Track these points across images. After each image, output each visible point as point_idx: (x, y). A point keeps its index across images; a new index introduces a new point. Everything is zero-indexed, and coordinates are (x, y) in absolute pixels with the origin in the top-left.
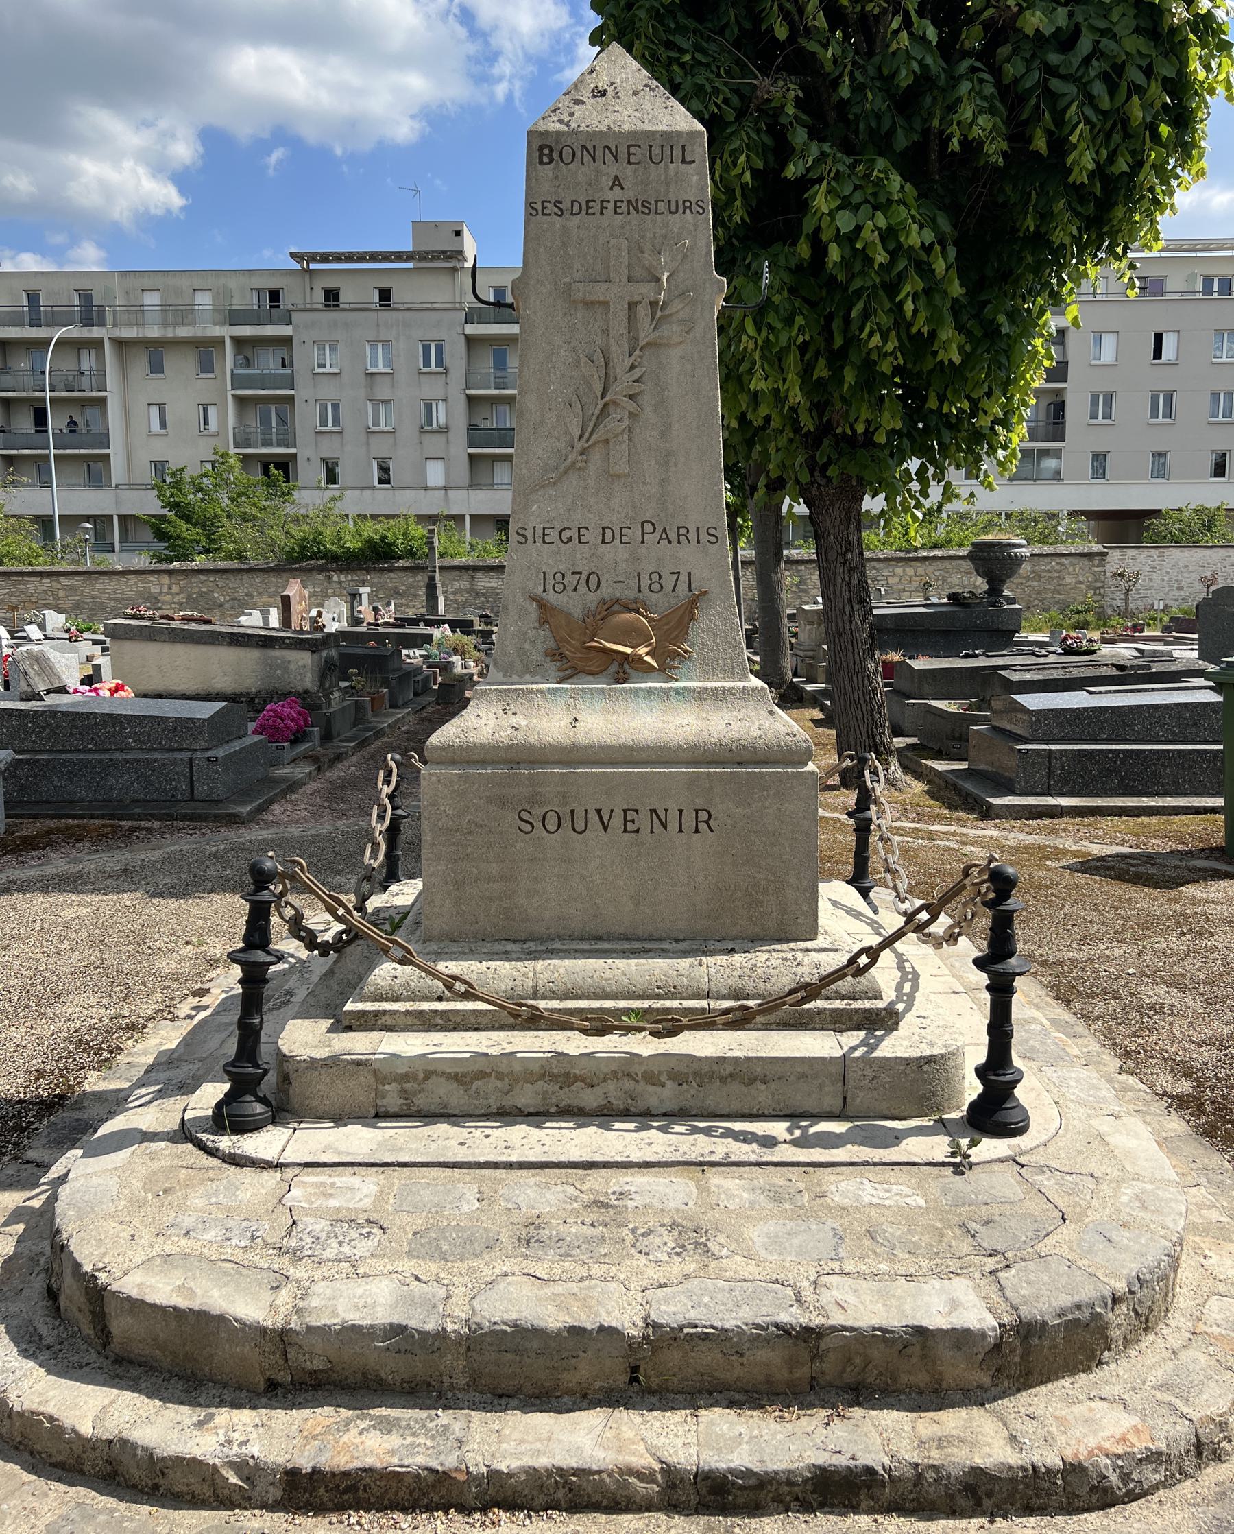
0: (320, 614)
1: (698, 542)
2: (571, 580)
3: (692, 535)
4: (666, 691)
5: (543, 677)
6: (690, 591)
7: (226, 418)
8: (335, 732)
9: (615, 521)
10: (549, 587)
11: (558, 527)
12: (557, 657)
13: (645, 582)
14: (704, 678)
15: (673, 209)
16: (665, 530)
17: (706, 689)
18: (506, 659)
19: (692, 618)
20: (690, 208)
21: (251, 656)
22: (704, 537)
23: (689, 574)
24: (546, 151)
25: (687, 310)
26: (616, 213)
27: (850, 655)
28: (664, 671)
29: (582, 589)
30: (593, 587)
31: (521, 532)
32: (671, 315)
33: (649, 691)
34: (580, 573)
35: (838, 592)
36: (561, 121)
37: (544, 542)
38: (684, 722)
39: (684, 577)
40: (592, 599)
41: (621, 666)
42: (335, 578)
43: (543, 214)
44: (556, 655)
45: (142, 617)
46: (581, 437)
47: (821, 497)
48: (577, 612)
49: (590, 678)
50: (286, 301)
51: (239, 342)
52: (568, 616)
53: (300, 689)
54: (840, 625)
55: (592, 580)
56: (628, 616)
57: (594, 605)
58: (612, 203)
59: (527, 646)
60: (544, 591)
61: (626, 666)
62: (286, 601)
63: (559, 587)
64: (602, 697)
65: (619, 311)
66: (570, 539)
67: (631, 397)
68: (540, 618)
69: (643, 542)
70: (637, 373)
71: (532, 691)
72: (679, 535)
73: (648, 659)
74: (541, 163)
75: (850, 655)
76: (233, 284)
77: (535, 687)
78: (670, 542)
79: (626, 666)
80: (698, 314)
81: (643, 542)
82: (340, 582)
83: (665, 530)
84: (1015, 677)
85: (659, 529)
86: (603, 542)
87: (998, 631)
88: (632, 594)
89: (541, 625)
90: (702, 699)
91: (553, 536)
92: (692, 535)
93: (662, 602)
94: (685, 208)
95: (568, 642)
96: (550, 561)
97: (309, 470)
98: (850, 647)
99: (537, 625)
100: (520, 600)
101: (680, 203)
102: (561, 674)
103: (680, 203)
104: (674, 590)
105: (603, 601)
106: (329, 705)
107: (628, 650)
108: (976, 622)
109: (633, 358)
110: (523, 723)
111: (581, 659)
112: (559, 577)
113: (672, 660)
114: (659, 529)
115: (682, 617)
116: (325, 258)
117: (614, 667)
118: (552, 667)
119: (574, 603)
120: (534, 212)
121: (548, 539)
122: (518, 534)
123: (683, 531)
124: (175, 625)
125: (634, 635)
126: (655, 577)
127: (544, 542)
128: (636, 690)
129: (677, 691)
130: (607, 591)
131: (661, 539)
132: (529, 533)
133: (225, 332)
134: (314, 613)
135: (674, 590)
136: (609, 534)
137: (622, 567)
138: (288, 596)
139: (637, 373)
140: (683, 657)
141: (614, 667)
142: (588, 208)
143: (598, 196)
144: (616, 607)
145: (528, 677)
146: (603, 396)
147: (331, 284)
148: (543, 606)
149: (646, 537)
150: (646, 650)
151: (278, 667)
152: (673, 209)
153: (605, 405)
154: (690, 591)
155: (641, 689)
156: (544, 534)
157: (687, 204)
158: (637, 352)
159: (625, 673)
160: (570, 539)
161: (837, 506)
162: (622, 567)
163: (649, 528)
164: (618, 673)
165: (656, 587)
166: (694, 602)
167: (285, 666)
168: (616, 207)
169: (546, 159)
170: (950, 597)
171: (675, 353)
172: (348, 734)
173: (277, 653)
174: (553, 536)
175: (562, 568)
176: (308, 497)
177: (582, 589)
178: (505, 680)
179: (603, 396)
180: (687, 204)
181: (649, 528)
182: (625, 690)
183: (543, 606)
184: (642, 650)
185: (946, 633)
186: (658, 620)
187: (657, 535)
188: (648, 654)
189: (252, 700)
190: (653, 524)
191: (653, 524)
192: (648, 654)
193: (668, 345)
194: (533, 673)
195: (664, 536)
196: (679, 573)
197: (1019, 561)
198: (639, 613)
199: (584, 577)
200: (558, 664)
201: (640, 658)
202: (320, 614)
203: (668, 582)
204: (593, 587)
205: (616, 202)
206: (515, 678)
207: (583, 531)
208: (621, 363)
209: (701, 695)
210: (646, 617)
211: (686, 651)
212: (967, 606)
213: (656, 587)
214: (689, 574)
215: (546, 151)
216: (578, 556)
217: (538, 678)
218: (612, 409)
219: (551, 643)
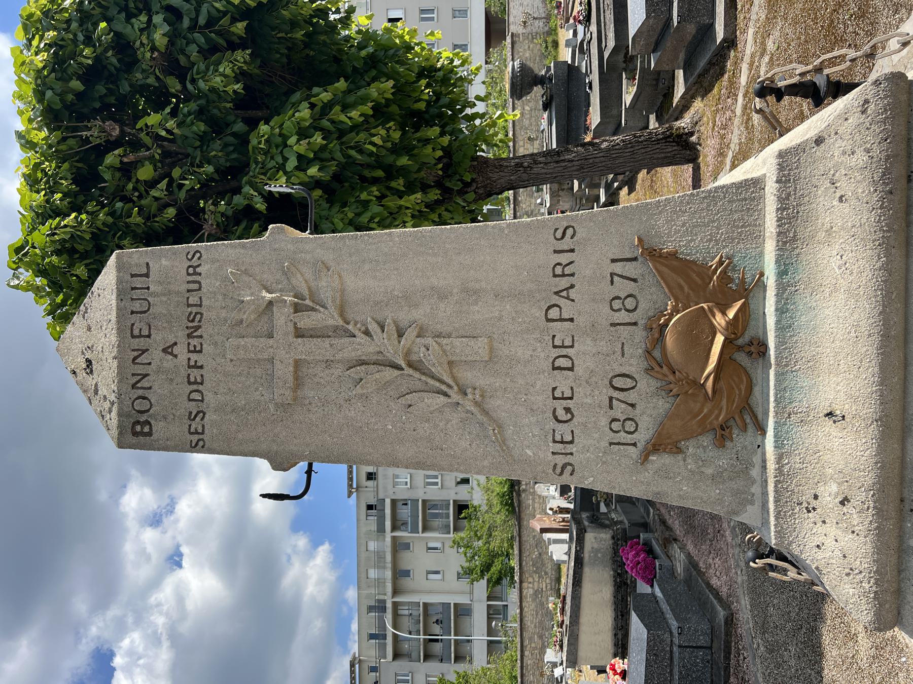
0: (551, 509)
1: (572, 251)
2: (620, 410)
3: (564, 258)
4: (782, 288)
5: (755, 452)
6: (635, 259)
7: (434, 538)
8: (642, 521)
9: (546, 354)
10: (629, 438)
11: (552, 424)
12: (726, 433)
13: (623, 317)
14: (758, 238)
15: (196, 286)
16: (556, 293)
17: (779, 234)
18: (728, 499)
19: (674, 255)
20: (195, 267)
21: (587, 572)
22: (565, 244)
23: (613, 261)
24: (138, 428)
25: (304, 270)
26: (200, 351)
27: (597, 160)
28: (747, 290)
29: (631, 397)
30: (629, 383)
31: (558, 470)
32: (309, 288)
33: (781, 311)
34: (611, 399)
35: (551, 171)
36: (110, 411)
37: (571, 442)
38: (835, 262)
39: (618, 268)
40: (646, 384)
41: (740, 348)
42: (524, 487)
43: (203, 433)
44: (722, 435)
45: (561, 641)
46: (446, 395)
47: (485, 187)
48: (662, 405)
49: (757, 390)
50: (372, 502)
51: (394, 528)
52: (669, 416)
53: (611, 542)
54: (575, 168)
55: (621, 384)
56: (670, 339)
57: (654, 383)
58: (191, 355)
59: (709, 471)
60: (635, 445)
61: (740, 342)
62: (544, 530)
63: (630, 426)
64: (790, 376)
65: (305, 348)
66: (568, 410)
67: (400, 335)
68: (671, 452)
69: (572, 320)
70: (373, 327)
71: (779, 470)
72: (563, 275)
73: (731, 314)
74: (150, 434)
75: (597, 160)
76: (364, 530)
77: (771, 466)
78: (572, 286)
79: (740, 342)
80: (308, 257)
81: (572, 320)
82: (526, 484)
83: (556, 293)
84: (611, 44)
85: (556, 300)
86: (571, 369)
87: (568, 75)
88: (639, 334)
89: (679, 451)
90: (794, 239)
91: (563, 431)
92: (564, 258)
93: (652, 296)
94: (195, 273)
95: (706, 417)
96: (596, 436)
97: (462, 494)
98: (591, 161)
99: (680, 457)
100: (647, 475)
101: (190, 278)
102: (751, 428)
103: (190, 278)
104: (635, 280)
105: (649, 370)
106: (621, 522)
107: (719, 339)
108: (563, 92)
109: (357, 333)
110: (834, 488)
111: (730, 400)
112: (616, 426)
113: (731, 280)
114: (556, 300)
115: (673, 269)
116: (350, 479)
117: (741, 358)
118: (741, 440)
119: (651, 408)
120: (201, 443)
121: (568, 438)
122: (561, 474)
123: (559, 270)
124: (567, 621)
125: (697, 334)
126: (617, 304)
127: (571, 442)
128: (781, 328)
129: (781, 273)
130: (634, 364)
131: (568, 298)
132: (561, 460)
133: (389, 535)
134: (551, 512)
135: (635, 280)
136: (562, 362)
137: (603, 346)
138: (541, 529)
139: (373, 327)
140: (727, 264)
141: (741, 358)
142: (195, 383)
143: (183, 372)
144: (657, 354)
145: (755, 472)
146: (399, 368)
147: (364, 476)
148: (656, 447)
149: (565, 315)
150: (719, 316)
151: (596, 555)
152: (196, 286)
153: (410, 365)
154: (635, 259)
155: (778, 322)
156: (562, 442)
157: (191, 270)
158: (350, 327)
159: (751, 343)
160: (568, 410)
161: (491, 175)
162: (603, 346)
163: (554, 313)
164: (750, 354)
165: (630, 303)
166: (653, 254)
167: (595, 551)
168: (195, 351)
169: (146, 429)
170: (545, 110)
171: (351, 283)
172: (642, 510)
173: (586, 556)
174: (563, 431)
175: (604, 422)
176: (477, 497)
177: (631, 397)
178: (758, 504)
179: (399, 368)
180: (191, 270)
181: (554, 313)
182: (781, 342)
183: (656, 447)
184: (719, 320)
185: (569, 110)
186: (676, 300)
187: (562, 302)
188: (724, 314)
189: (618, 574)
190: (549, 308)
191: (549, 308)
192: (724, 314)
193: (343, 291)
194: (749, 465)
195: (564, 294)
196: (612, 275)
197: (523, 66)
198: (666, 325)
199: (616, 394)
200: (735, 431)
201: (733, 325)
202: (551, 509)
203: (623, 288)
204: (629, 383)
205: (189, 351)
206: (756, 489)
207: (558, 394)
208: (362, 347)
209: (788, 240)
210: (671, 316)
211: (721, 263)
212: (552, 97)
213: (630, 303)
214: (613, 261)
215: (138, 428)
216: (589, 400)
217: (757, 459)
218: (414, 357)
219: (706, 440)
